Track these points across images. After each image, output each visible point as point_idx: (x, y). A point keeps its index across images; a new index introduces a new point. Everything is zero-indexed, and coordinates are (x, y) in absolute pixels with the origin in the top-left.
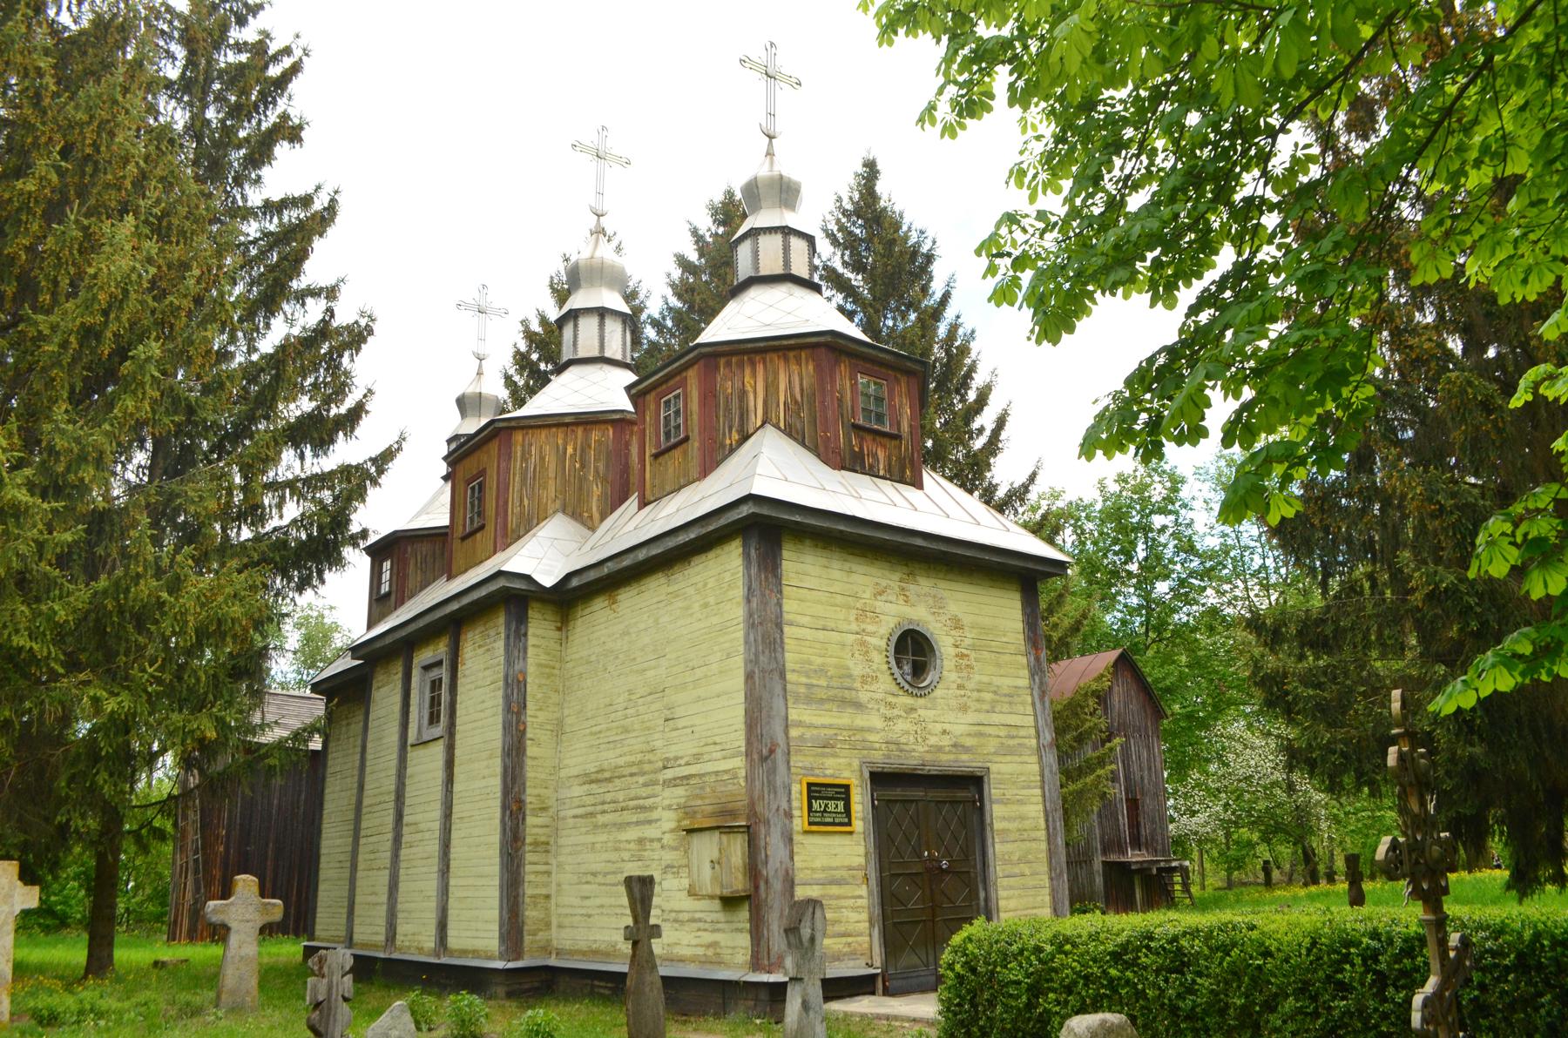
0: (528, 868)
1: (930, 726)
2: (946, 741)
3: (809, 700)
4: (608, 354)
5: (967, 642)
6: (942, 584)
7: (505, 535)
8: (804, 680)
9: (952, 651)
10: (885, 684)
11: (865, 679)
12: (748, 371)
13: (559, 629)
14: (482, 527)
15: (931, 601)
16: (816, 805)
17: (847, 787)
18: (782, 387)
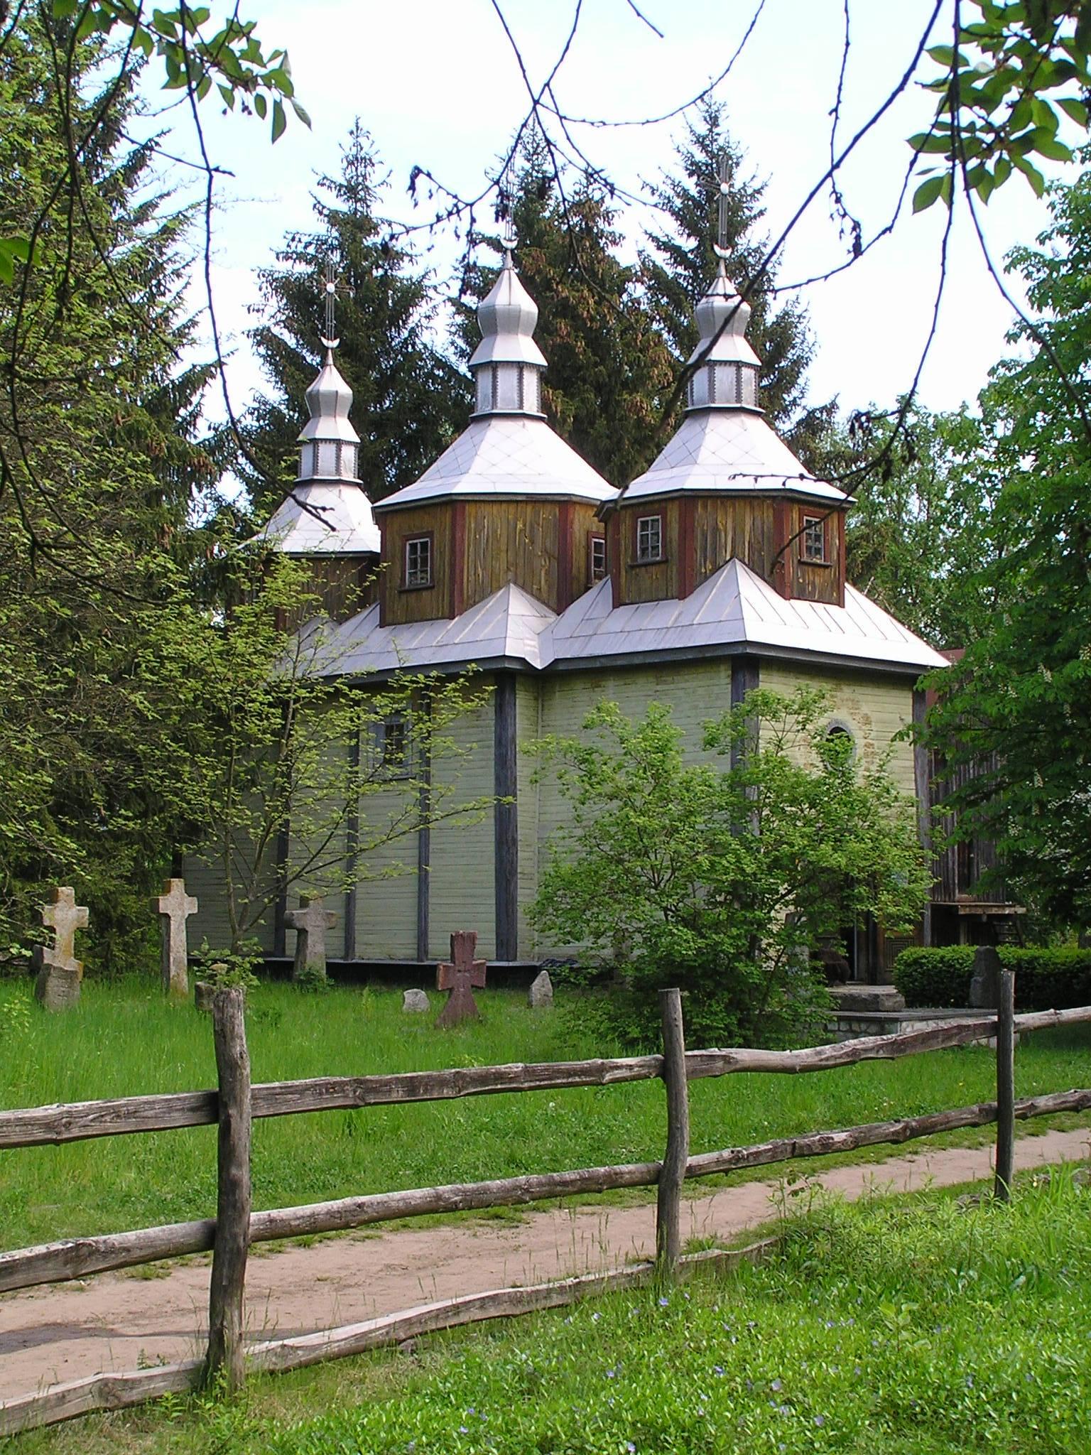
0: (519, 891)
4: (526, 410)
5: (873, 734)
6: (859, 690)
7: (462, 602)
14: (433, 587)
18: (747, 528)
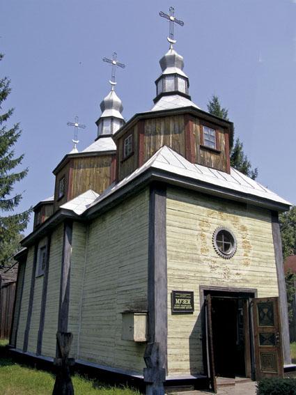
0: (69, 326)
1: (231, 271)
2: (237, 278)
3: (177, 257)
8: (175, 250)
9: (242, 240)
10: (212, 254)
11: (202, 250)
12: (157, 124)
13: (85, 232)
15: (233, 219)
16: (177, 301)
17: (192, 293)
